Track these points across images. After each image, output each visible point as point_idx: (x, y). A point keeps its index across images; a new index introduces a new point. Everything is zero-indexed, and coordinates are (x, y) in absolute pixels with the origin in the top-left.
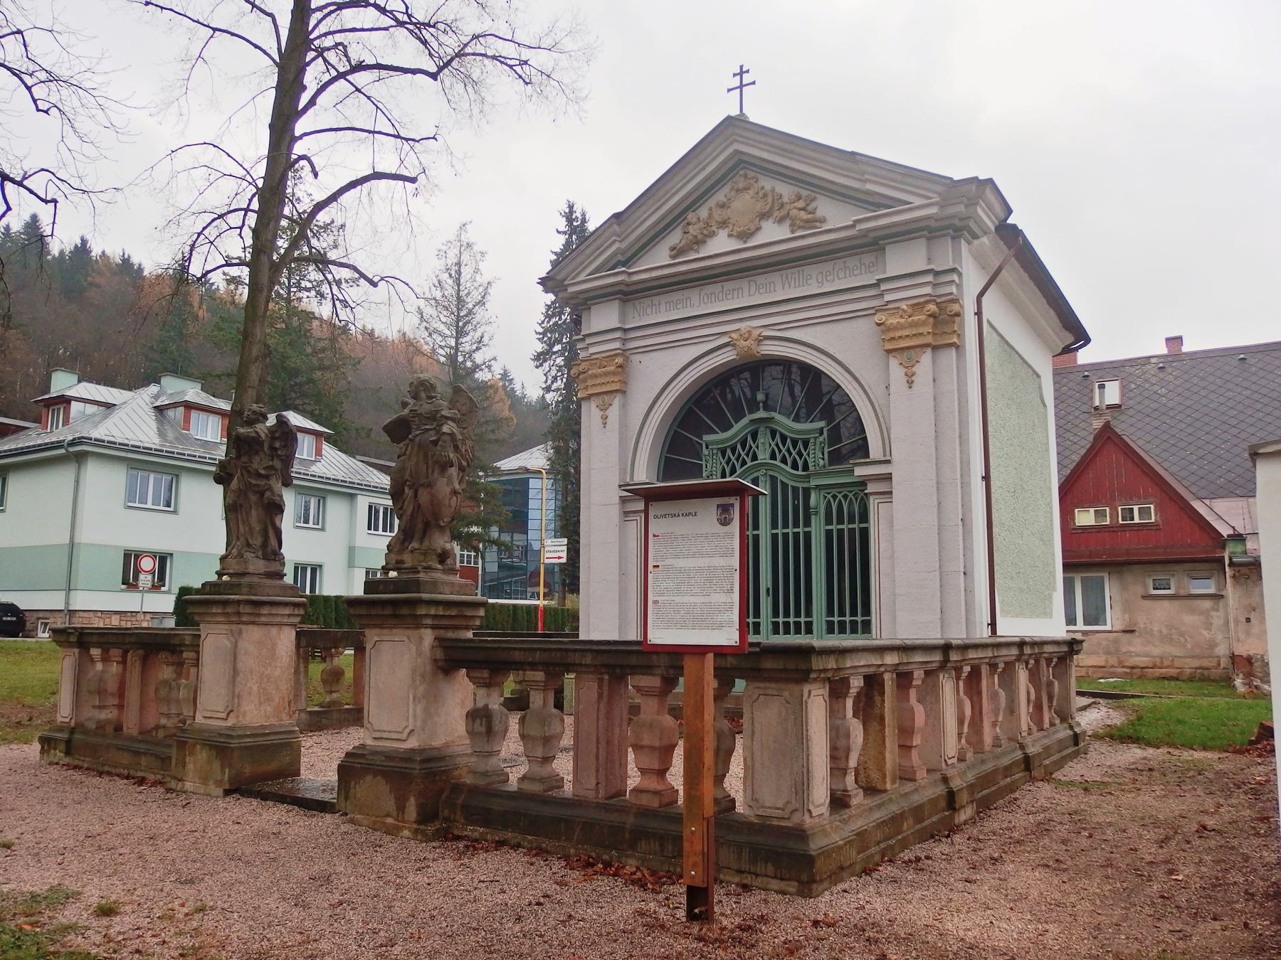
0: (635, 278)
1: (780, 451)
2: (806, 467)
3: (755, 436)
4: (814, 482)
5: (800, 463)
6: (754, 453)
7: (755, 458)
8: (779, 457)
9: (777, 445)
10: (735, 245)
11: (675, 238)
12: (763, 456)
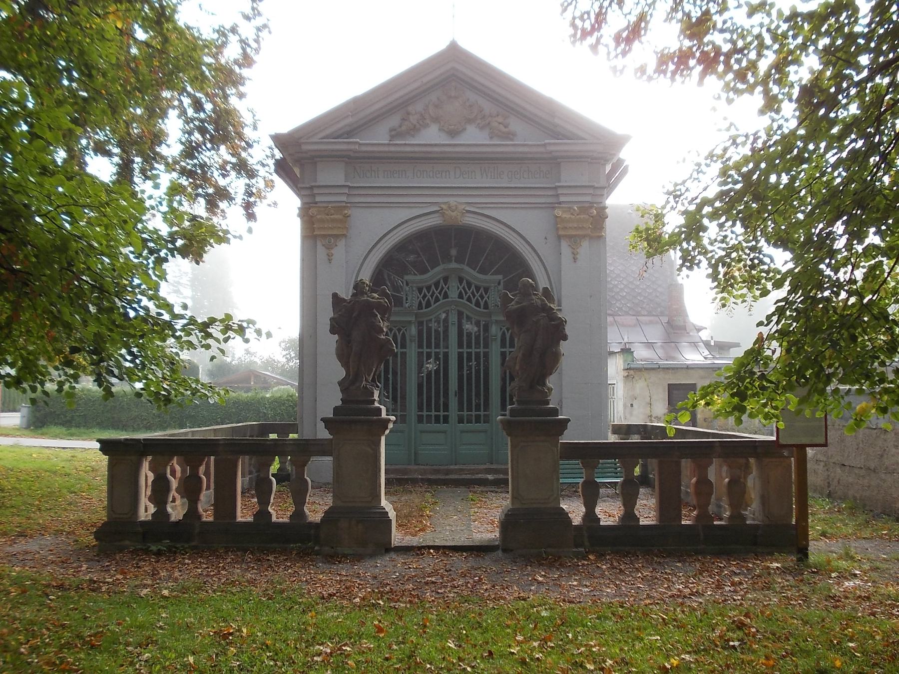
0: (364, 149)
1: (466, 293)
2: (486, 306)
3: (446, 279)
4: (494, 318)
5: (482, 304)
6: (446, 292)
7: (446, 296)
8: (465, 297)
9: (464, 288)
10: (444, 139)
11: (394, 121)
12: (453, 295)
